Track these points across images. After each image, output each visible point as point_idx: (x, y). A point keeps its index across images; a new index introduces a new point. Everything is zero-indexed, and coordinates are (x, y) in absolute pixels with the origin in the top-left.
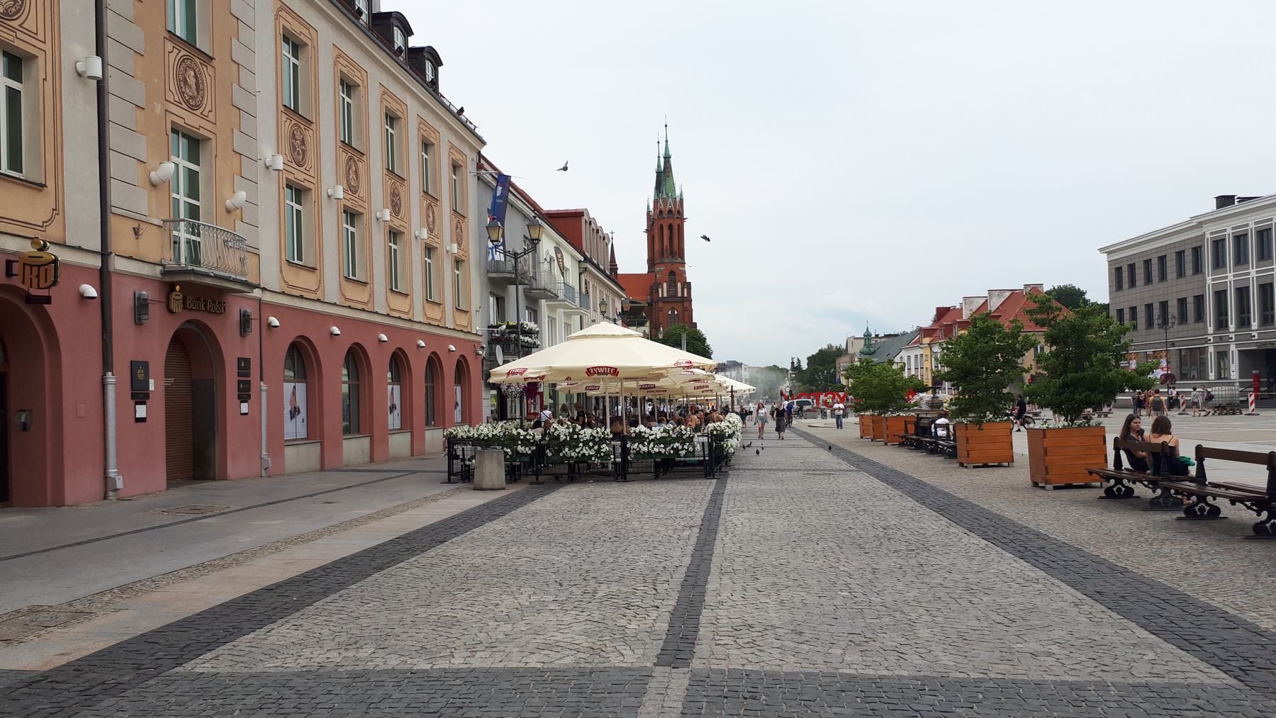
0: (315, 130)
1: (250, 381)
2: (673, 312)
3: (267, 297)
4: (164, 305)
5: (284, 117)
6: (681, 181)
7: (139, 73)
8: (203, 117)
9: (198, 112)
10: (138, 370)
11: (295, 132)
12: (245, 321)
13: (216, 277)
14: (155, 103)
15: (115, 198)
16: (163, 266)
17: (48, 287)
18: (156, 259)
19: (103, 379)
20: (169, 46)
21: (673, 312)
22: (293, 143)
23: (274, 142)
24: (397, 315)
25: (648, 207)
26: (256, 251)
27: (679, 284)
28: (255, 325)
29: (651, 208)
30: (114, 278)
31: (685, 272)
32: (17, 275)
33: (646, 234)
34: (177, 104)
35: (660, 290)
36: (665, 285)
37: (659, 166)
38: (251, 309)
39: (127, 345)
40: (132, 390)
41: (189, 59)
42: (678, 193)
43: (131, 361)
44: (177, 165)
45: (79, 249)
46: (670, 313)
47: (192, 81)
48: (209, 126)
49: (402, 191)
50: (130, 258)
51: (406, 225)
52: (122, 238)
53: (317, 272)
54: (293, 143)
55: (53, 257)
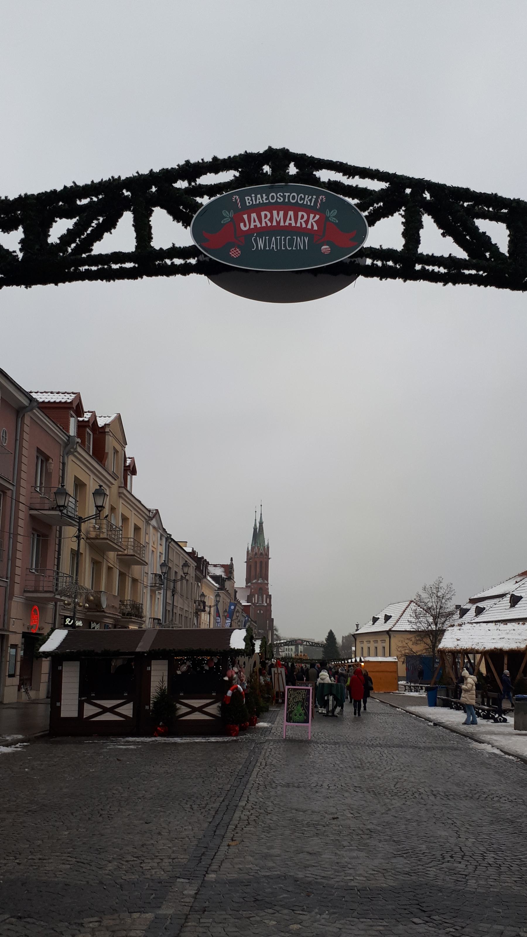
2: (260, 612)
6: (268, 536)
21: (260, 612)
25: (248, 549)
27: (265, 596)
29: (250, 549)
31: (268, 589)
33: (246, 564)
35: (253, 599)
36: (256, 596)
37: (255, 525)
42: (266, 543)
46: (258, 612)
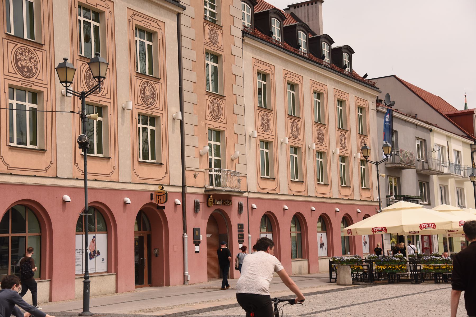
0: (274, 113)
1: (243, 234)
3: (251, 195)
4: (206, 204)
5: (258, 111)
7: (195, 112)
8: (221, 122)
9: (219, 121)
10: (196, 231)
11: (264, 117)
12: (241, 208)
13: (226, 191)
14: (202, 122)
15: (187, 164)
16: (205, 188)
17: (164, 203)
18: (202, 186)
19: (183, 236)
20: (207, 96)
22: (263, 122)
23: (253, 125)
24: (321, 196)
26: (246, 176)
28: (245, 209)
30: (187, 195)
32: (154, 199)
34: (210, 120)
38: (243, 202)
39: (192, 222)
40: (194, 240)
41: (215, 100)
43: (193, 228)
44: (210, 146)
45: (174, 186)
47: (216, 108)
48: (224, 125)
49: (324, 131)
50: (193, 187)
51: (327, 148)
52: (190, 180)
53: (276, 180)
54: (263, 122)
55: (165, 192)
